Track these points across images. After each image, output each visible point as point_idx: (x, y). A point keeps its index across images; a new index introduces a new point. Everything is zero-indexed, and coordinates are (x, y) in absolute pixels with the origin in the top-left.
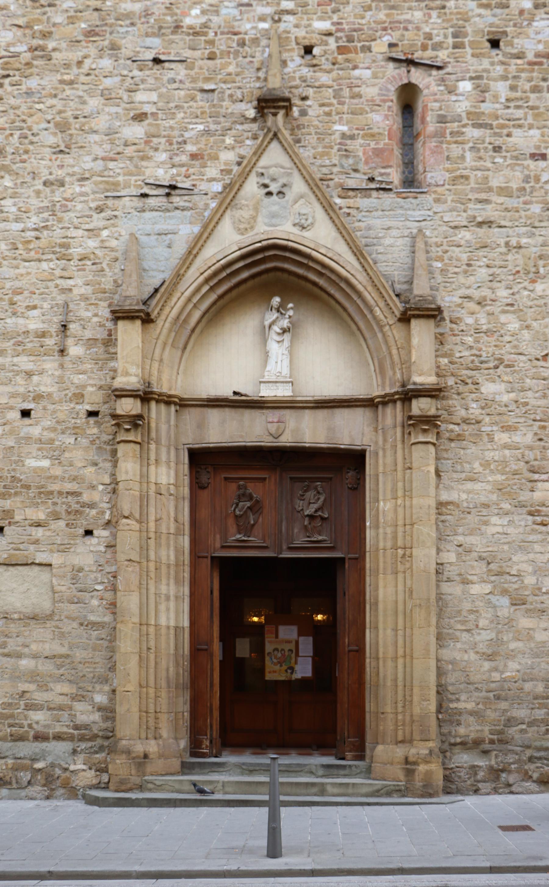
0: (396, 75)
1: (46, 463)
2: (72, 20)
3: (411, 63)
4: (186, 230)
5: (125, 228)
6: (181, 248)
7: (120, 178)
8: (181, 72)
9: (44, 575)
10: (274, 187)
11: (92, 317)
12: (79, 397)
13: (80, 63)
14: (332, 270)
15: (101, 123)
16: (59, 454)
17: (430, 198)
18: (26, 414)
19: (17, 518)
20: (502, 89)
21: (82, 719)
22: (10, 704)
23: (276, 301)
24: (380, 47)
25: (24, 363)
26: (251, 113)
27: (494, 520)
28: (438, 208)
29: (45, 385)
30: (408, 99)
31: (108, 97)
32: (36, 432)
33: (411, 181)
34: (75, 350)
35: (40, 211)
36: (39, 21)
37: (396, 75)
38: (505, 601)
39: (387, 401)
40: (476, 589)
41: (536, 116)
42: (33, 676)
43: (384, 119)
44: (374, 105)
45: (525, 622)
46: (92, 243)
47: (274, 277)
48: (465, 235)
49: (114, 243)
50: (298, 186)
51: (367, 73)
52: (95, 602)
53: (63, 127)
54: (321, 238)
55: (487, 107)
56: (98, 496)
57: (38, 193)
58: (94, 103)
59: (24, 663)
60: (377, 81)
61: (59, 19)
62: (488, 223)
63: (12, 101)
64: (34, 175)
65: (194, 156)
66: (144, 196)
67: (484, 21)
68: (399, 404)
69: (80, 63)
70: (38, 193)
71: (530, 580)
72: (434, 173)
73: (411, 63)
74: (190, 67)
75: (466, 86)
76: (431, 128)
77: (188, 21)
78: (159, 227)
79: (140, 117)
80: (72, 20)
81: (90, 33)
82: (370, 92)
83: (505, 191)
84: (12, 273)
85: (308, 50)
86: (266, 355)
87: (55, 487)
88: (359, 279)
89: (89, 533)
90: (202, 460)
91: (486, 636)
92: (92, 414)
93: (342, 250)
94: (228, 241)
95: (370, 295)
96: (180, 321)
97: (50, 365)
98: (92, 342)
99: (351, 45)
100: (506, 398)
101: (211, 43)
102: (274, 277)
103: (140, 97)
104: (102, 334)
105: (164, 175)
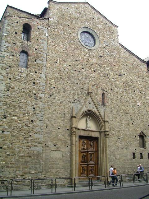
0: (102, 92)
1: (61, 136)
2: (66, 75)
3: (104, 90)
4: (79, 107)
5: (72, 105)
6: (79, 108)
7: (71, 98)
8: (79, 86)
9: (61, 153)
10: (90, 103)
11: (68, 116)
12: (66, 127)
13: (67, 81)
14: (96, 115)
15: (69, 89)
16: (64, 135)
17: (106, 107)
18: (59, 128)
19: (58, 144)
20: (113, 95)
21: (66, 174)
22: (56, 173)
23: (88, 117)
24: (101, 87)
25: (59, 121)
26: (87, 93)
27: (113, 148)
28: (107, 108)
29: (62, 125)
30: (103, 94)
31: (70, 86)
32: (60, 131)
33: (104, 104)
34: (66, 120)
35: (61, 100)
36: (61, 74)
37: (102, 92)
38: (114, 158)
39: (102, 132)
40: (112, 156)
41: (116, 99)
42: (59, 168)
43: (101, 96)
44: (100, 95)
45: (117, 161)
46: (68, 106)
47: (89, 114)
48: (110, 112)
49: (70, 106)
50: (93, 103)
51: (99, 90)
52: (68, 157)
53: (64, 89)
54: (95, 110)
55: (111, 97)
56: (69, 141)
57: (61, 97)
58: (68, 87)
59: (58, 166)
60: (100, 92)
61: (64, 74)
62: (112, 111)
63: (58, 84)
64: (61, 95)
65: (80, 97)
66: (74, 101)
67: (111, 87)
68: (104, 133)
69: (67, 81)
70: (61, 97)
71: (117, 155)
72: (106, 104)
73: (104, 90)
74: (80, 85)
75: (109, 94)
76: (106, 98)
77: (80, 79)
78: (77, 105)
79: (74, 90)
80: (66, 75)
81: (68, 77)
82: (100, 93)
83: (113, 108)
84: (57, 108)
85: (93, 86)
86: (87, 124)
87: (63, 139)
88: (99, 117)
89: (67, 147)
90: (81, 137)
91: (113, 162)
92: (68, 129)
93: (98, 113)
94: (85, 109)
95: (100, 118)
96: (79, 118)
97: (62, 122)
98: (68, 119)
99: (98, 87)
100: (114, 132)
101: (82, 82)
102: (89, 114)
103: (74, 87)
104: (69, 119)
105: (77, 98)
